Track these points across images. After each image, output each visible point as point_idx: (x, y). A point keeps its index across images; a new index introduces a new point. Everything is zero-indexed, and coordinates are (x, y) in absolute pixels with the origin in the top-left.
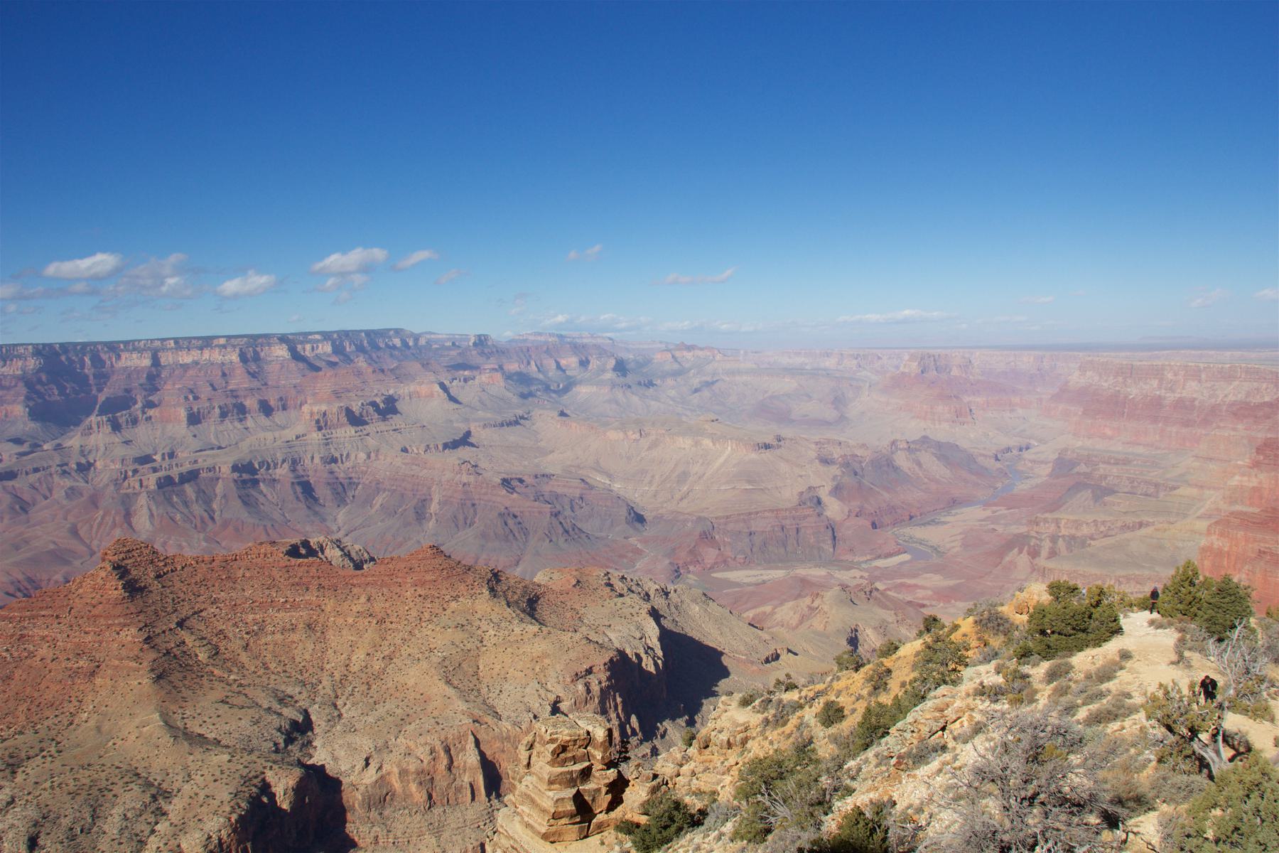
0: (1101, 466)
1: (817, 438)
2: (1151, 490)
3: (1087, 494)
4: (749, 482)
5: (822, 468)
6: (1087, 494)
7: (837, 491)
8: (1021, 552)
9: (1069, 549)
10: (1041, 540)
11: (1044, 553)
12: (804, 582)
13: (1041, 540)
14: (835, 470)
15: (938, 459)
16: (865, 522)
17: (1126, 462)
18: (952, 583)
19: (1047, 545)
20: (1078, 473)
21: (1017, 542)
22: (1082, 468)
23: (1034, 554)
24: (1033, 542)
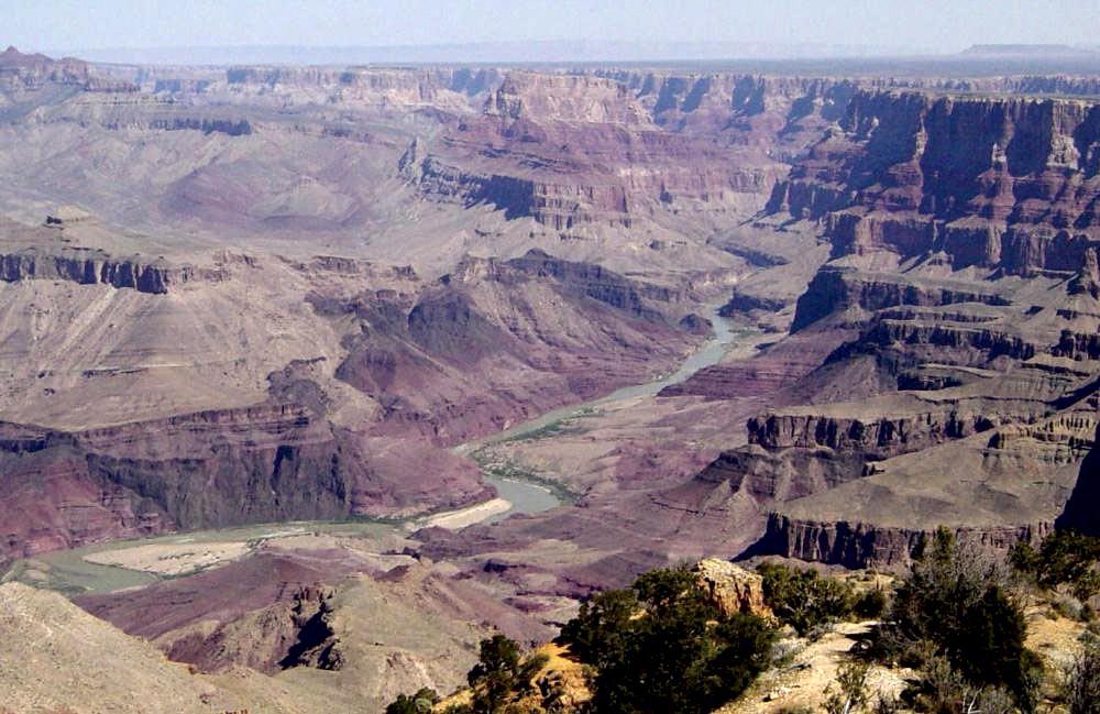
3: (869, 364)
5: (322, 323)
6: (869, 364)
8: (735, 488)
9: (832, 480)
11: (783, 490)
13: (774, 463)
17: (947, 298)
18: (594, 556)
19: (788, 472)
21: (731, 465)
23: (762, 492)
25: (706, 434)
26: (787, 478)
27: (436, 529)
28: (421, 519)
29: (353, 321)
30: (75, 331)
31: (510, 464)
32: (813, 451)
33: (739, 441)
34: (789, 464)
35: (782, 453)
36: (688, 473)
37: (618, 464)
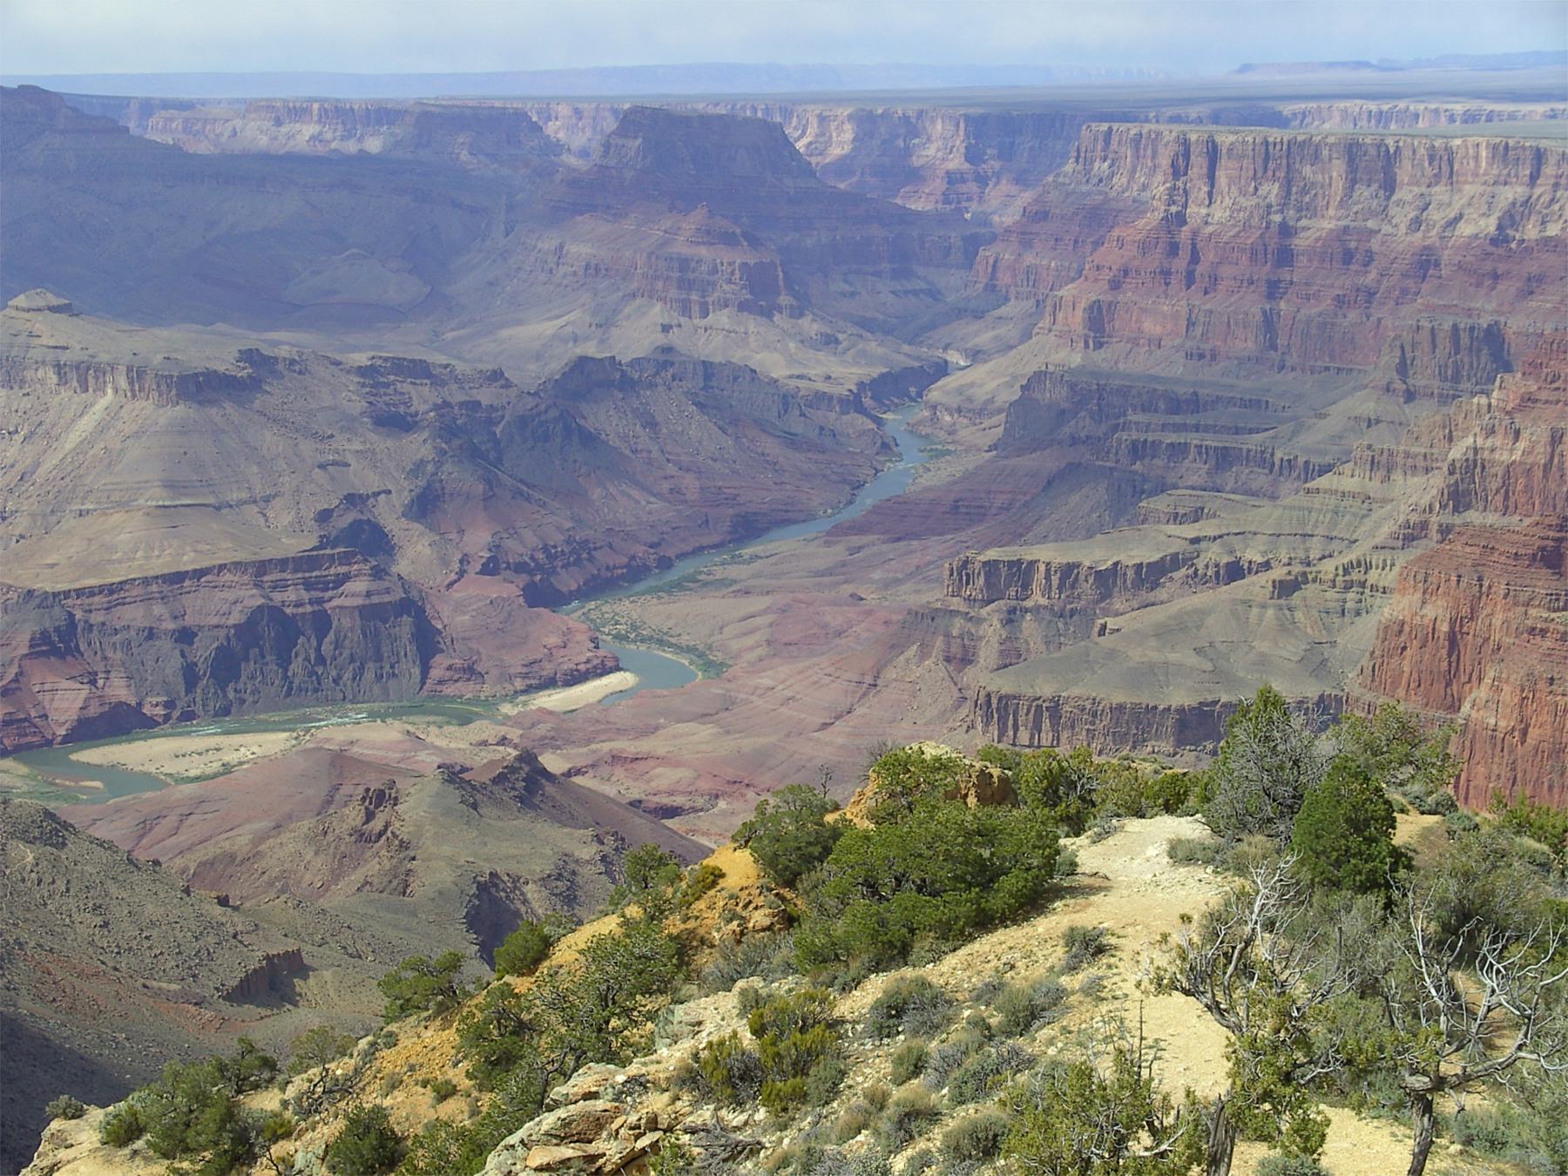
0: (1133, 417)
1: (362, 359)
2: (1261, 480)
4: (171, 486)
5: (383, 443)
7: (425, 506)
8: (923, 655)
10: (979, 621)
11: (987, 654)
12: (340, 761)
13: (979, 621)
14: (418, 446)
15: (701, 406)
16: (507, 589)
18: (748, 744)
20: (1074, 441)
22: (1083, 425)
24: (958, 625)
25: (886, 585)
26: (994, 641)
27: (541, 710)
28: (522, 698)
29: (425, 441)
30: (51, 461)
31: (634, 627)
32: (1029, 604)
33: (934, 596)
34: (996, 623)
35: (988, 608)
36: (865, 635)
37: (771, 625)
